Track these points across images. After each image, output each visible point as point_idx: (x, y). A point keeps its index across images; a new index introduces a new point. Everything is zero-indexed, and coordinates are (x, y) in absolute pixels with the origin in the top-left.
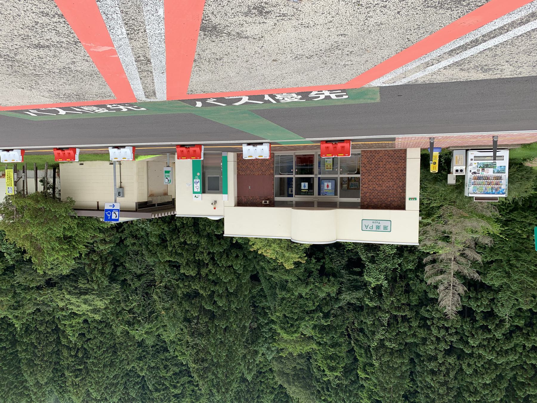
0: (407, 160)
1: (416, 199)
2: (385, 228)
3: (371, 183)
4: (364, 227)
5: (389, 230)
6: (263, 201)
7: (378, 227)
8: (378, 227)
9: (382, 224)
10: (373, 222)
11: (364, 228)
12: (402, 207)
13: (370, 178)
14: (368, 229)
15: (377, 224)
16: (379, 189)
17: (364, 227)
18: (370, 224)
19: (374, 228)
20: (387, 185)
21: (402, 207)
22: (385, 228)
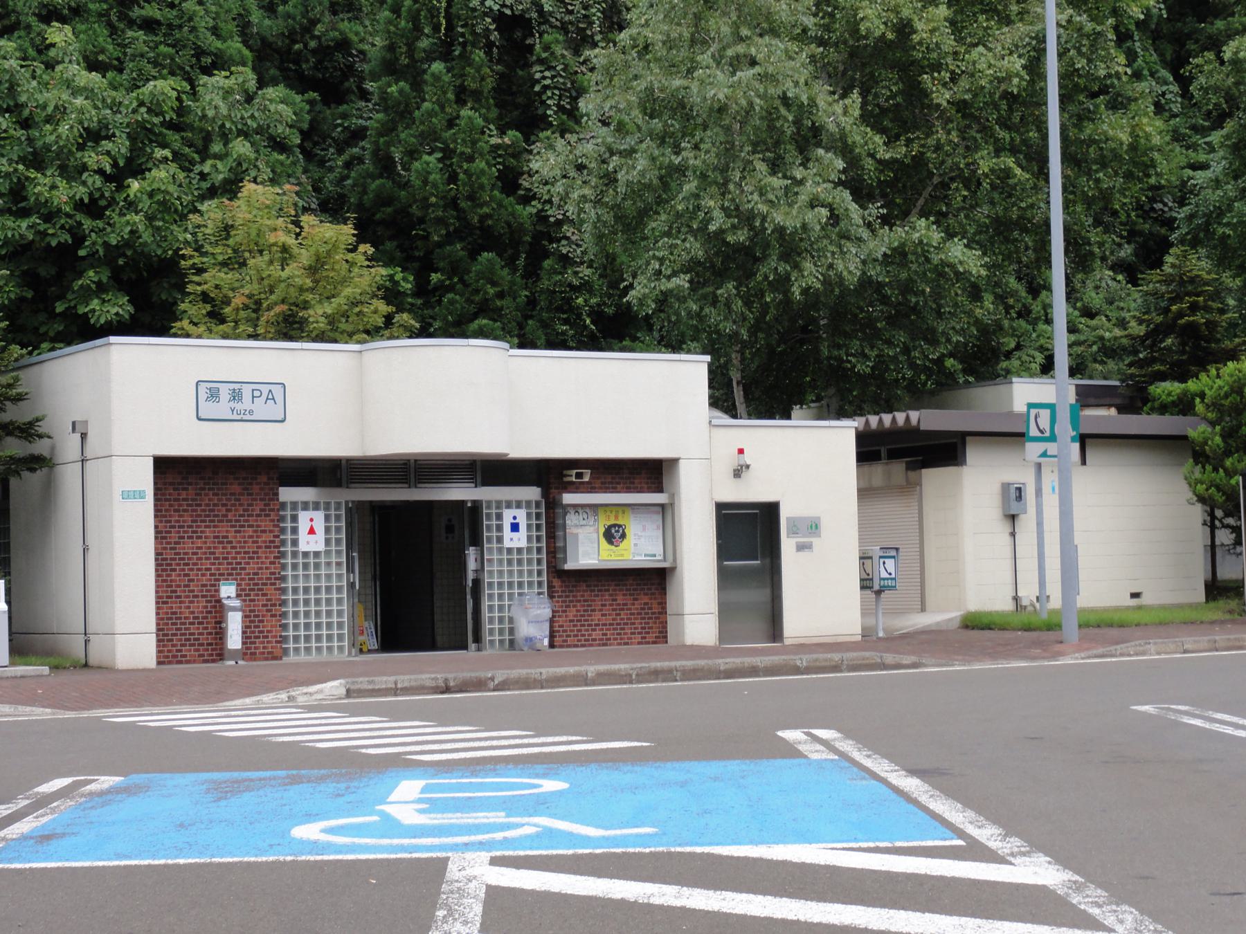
0: (153, 628)
1: (141, 495)
2: (214, 395)
3: (250, 547)
4: (279, 399)
5: (203, 387)
6: (586, 479)
7: (236, 396)
8: (236, 396)
9: (223, 407)
10: (251, 412)
11: (277, 391)
12: (173, 473)
13: (252, 567)
14: (265, 389)
15: (238, 406)
16: (223, 529)
17: (279, 399)
18: (261, 409)
19: (247, 391)
20: (199, 543)
21: (165, 467)
22: (214, 395)
